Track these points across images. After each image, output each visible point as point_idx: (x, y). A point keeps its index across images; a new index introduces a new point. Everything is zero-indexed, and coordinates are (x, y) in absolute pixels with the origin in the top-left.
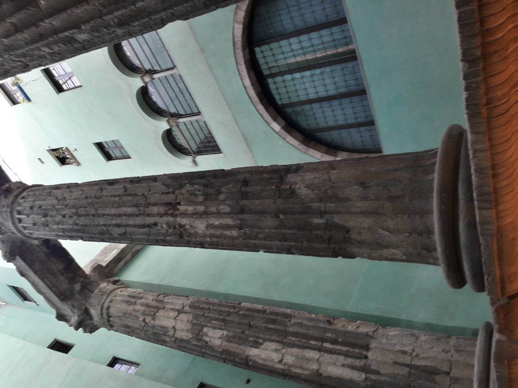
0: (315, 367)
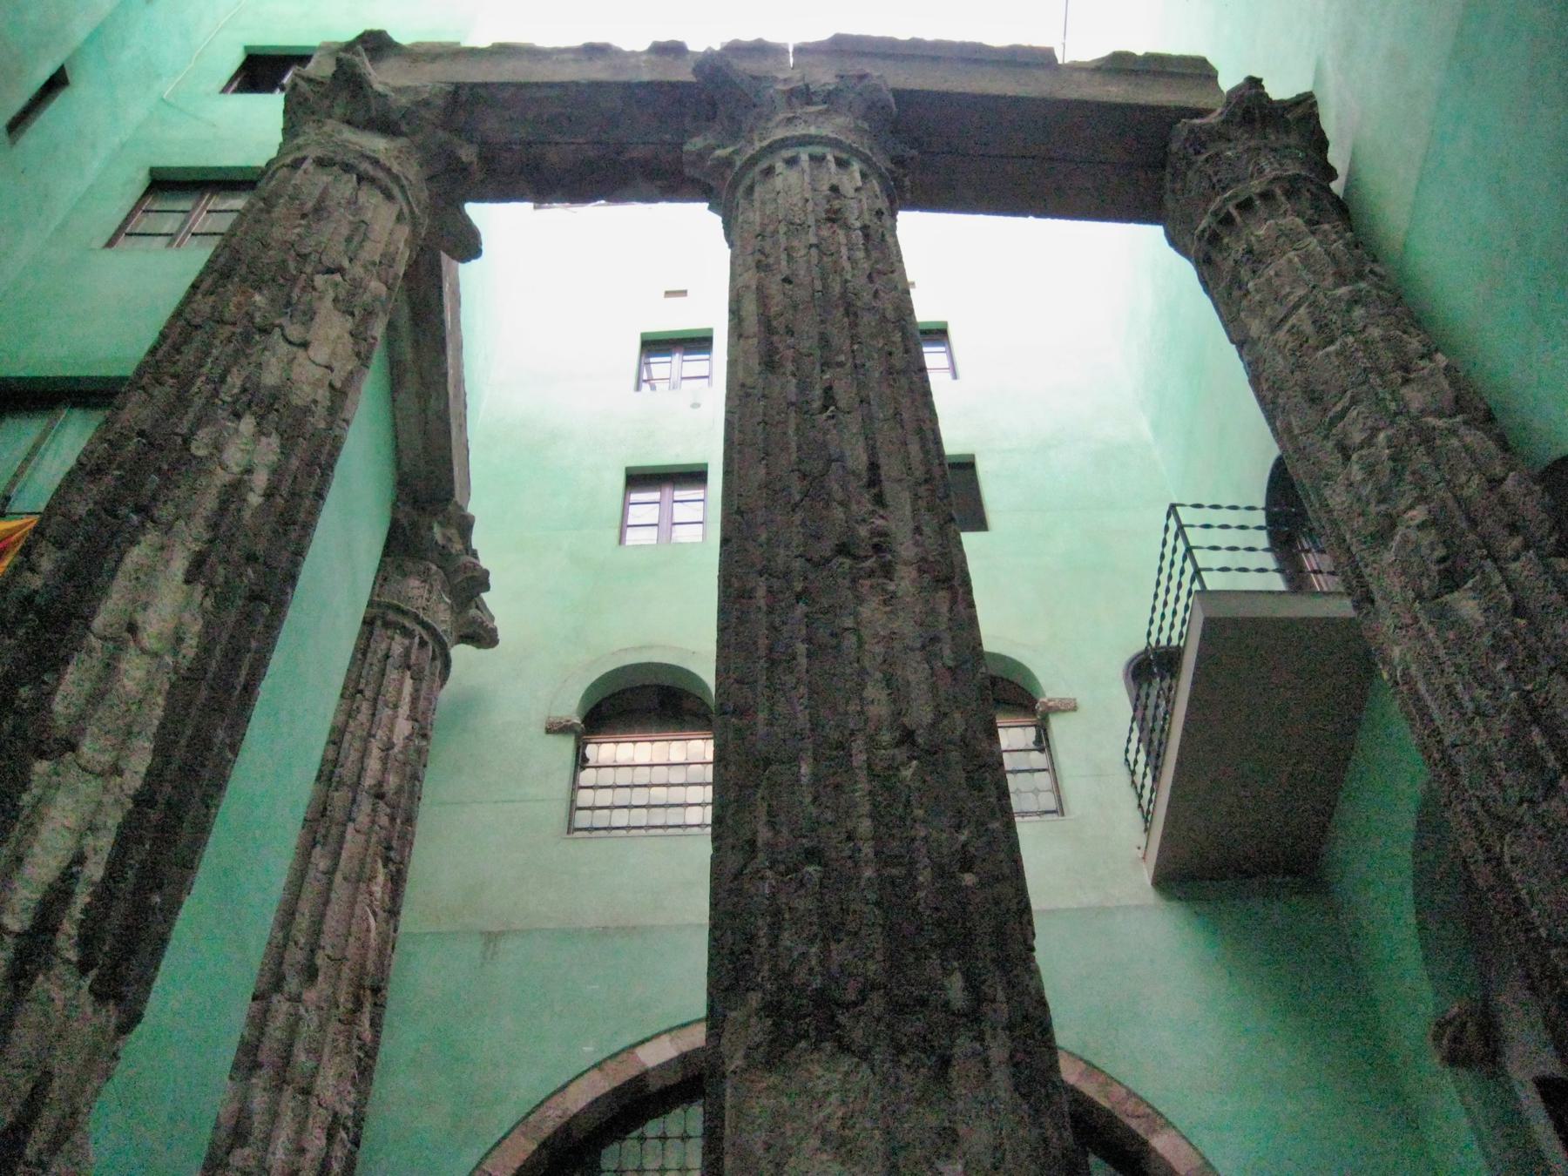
0: (92, 749)
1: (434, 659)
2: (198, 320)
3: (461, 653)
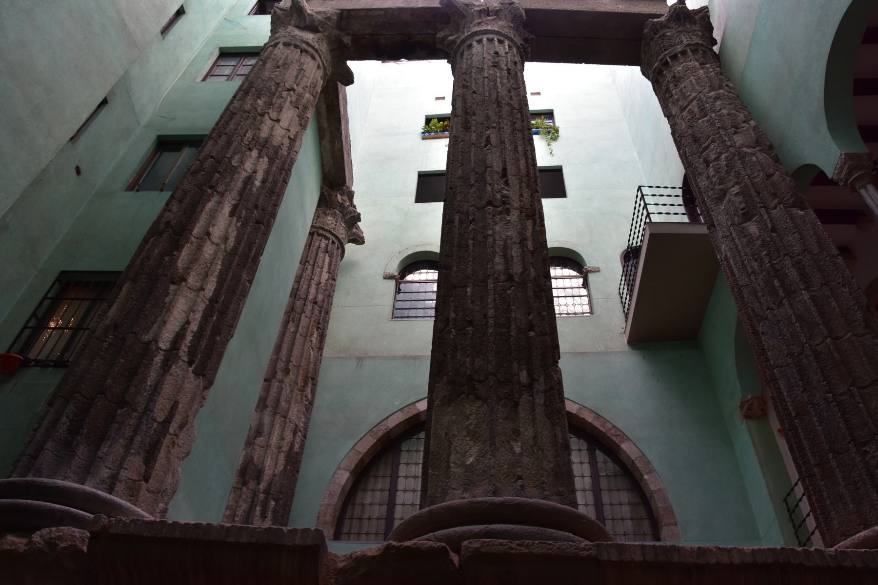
0: (191, 280)
1: (338, 248)
2: (235, 111)
3: (349, 247)
